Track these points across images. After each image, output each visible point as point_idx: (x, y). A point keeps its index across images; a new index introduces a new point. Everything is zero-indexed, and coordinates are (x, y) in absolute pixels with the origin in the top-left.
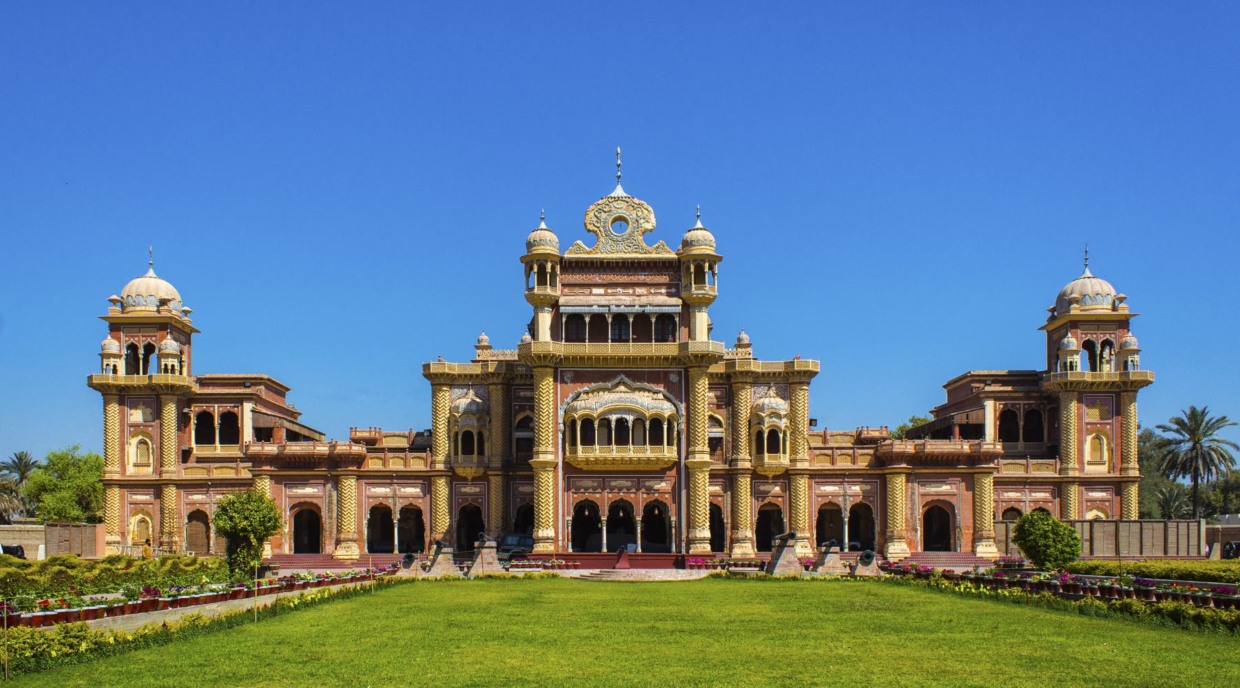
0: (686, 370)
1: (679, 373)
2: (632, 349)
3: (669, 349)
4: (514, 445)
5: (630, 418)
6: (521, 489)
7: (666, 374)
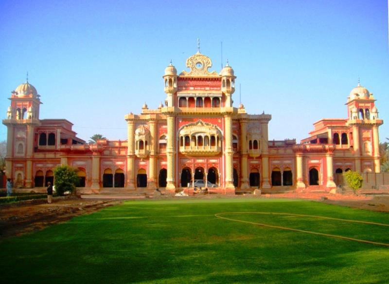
5: (203, 135)
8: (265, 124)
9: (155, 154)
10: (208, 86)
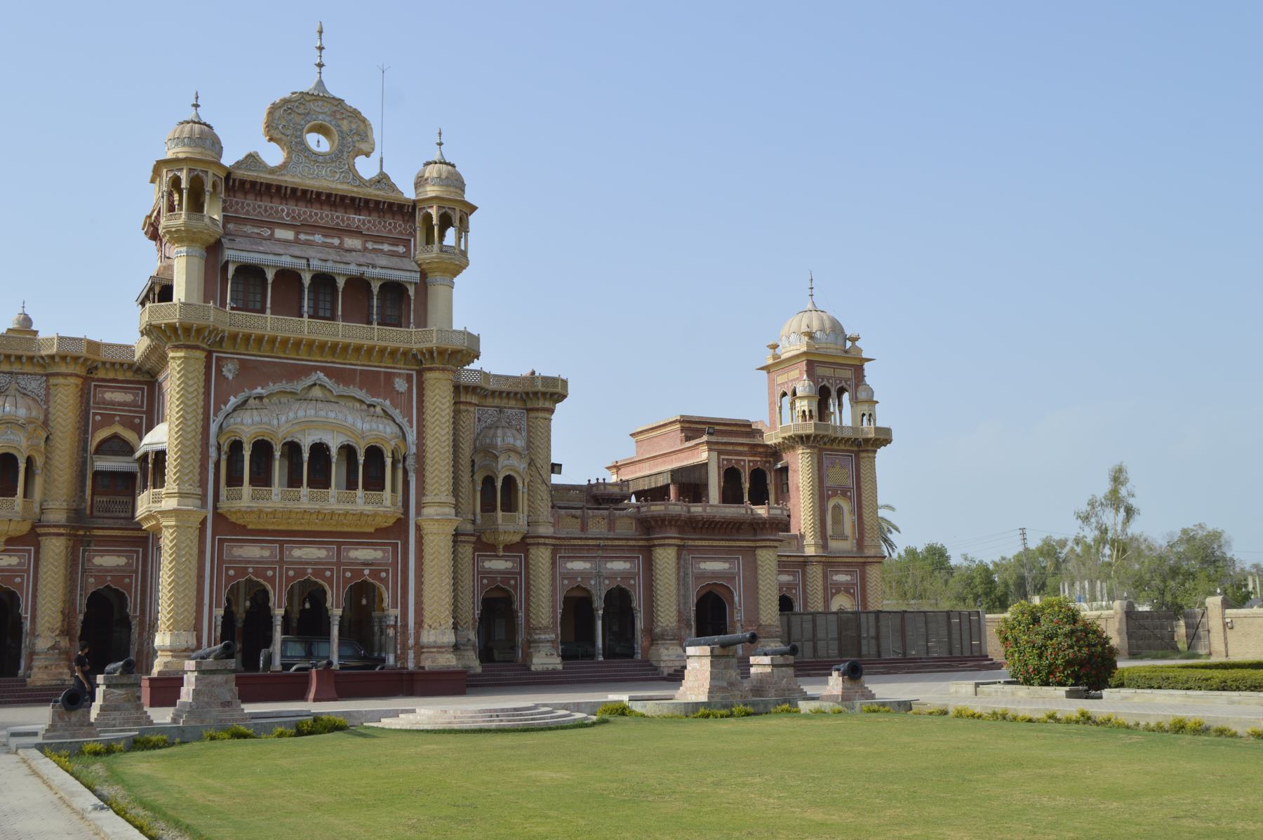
0: (420, 373)
1: (409, 378)
2: (342, 331)
3: (393, 337)
4: (89, 483)
6: (98, 561)
7: (389, 377)
8: (541, 415)
9: (68, 519)
10: (357, 233)
